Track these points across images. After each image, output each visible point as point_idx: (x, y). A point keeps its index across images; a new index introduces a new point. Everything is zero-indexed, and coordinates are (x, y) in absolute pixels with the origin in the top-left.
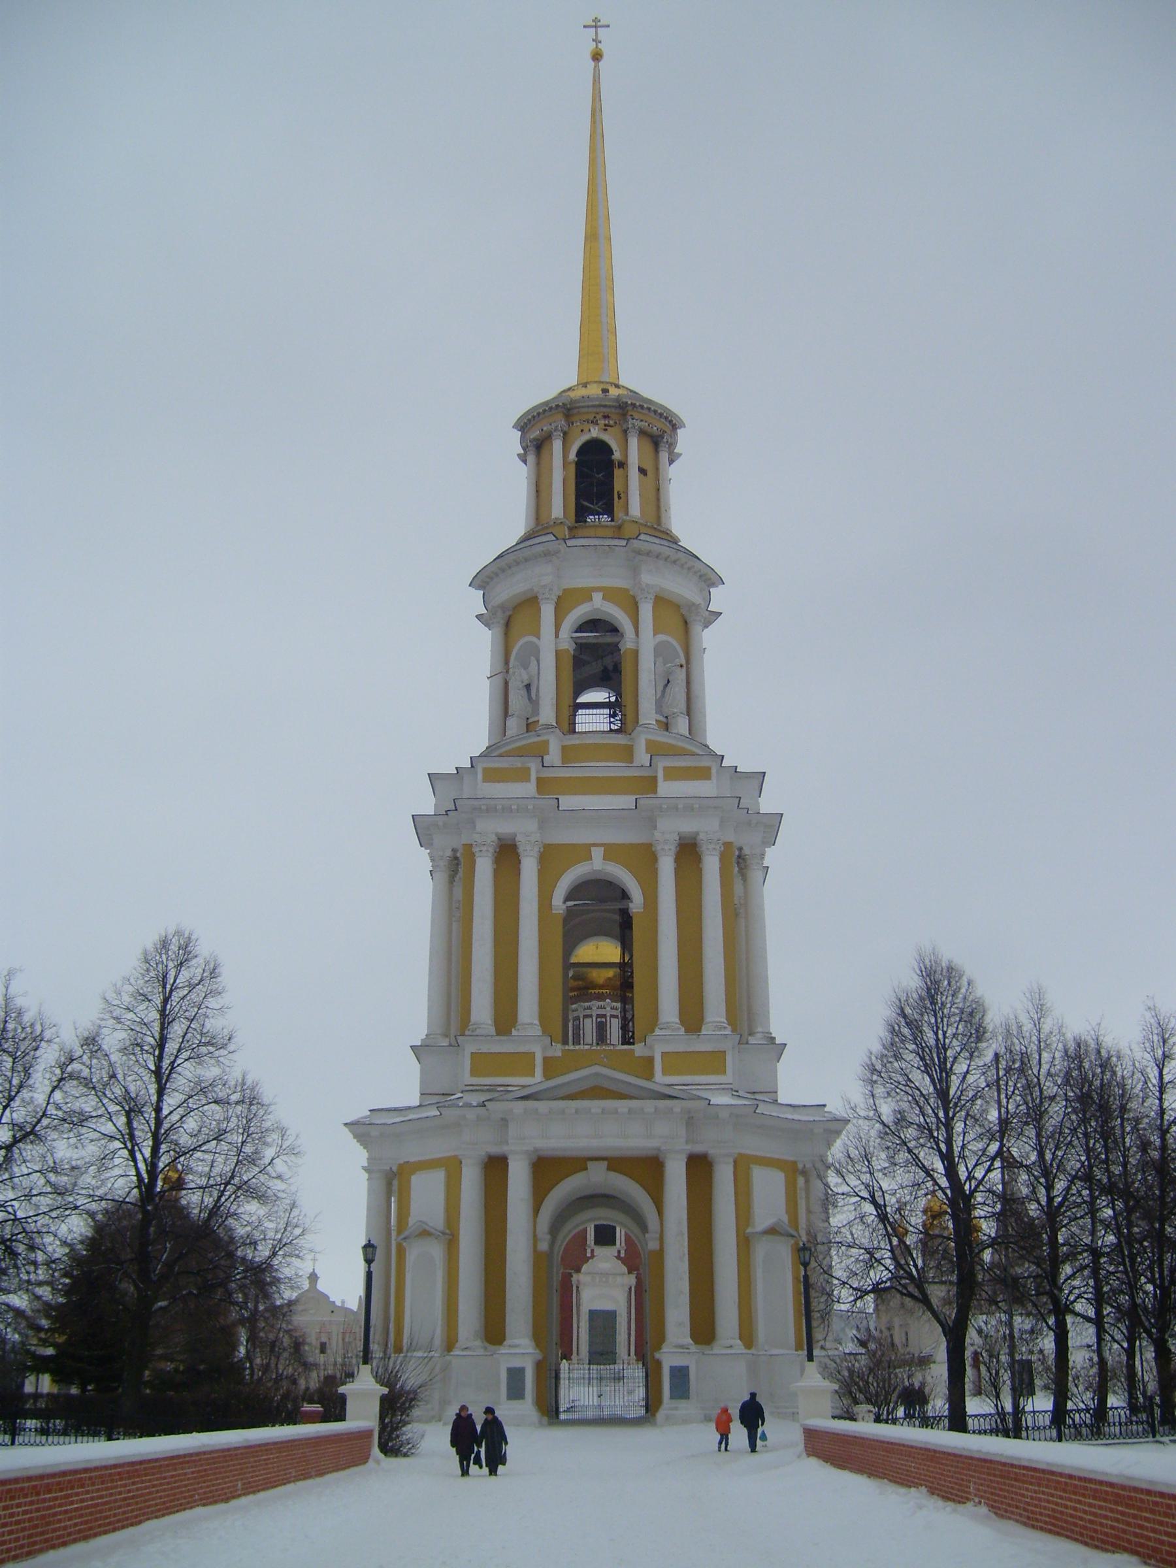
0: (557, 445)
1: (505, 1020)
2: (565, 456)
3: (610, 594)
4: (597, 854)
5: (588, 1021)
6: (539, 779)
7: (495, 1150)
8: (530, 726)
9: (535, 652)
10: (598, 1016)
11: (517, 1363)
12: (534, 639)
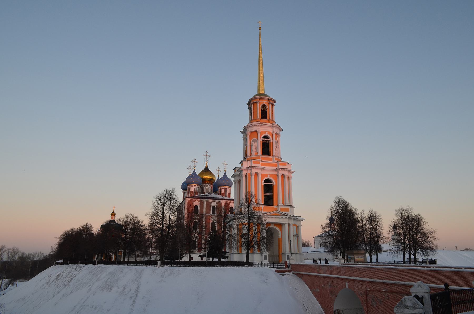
0: (258, 105)
2: (259, 107)
4: (269, 176)
5: (204, 188)
10: (206, 187)
11: (265, 255)
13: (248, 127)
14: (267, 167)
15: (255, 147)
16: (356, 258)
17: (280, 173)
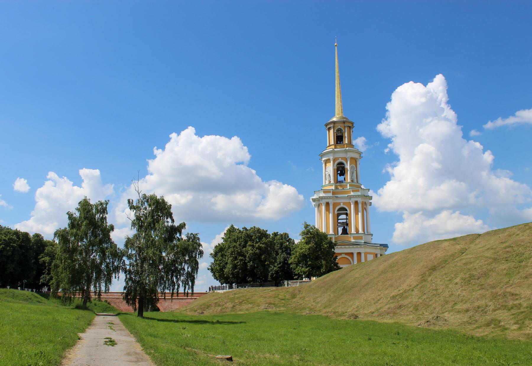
3: (342, 158)
4: (342, 204)
6: (332, 192)
12: (330, 167)
17: (353, 200)
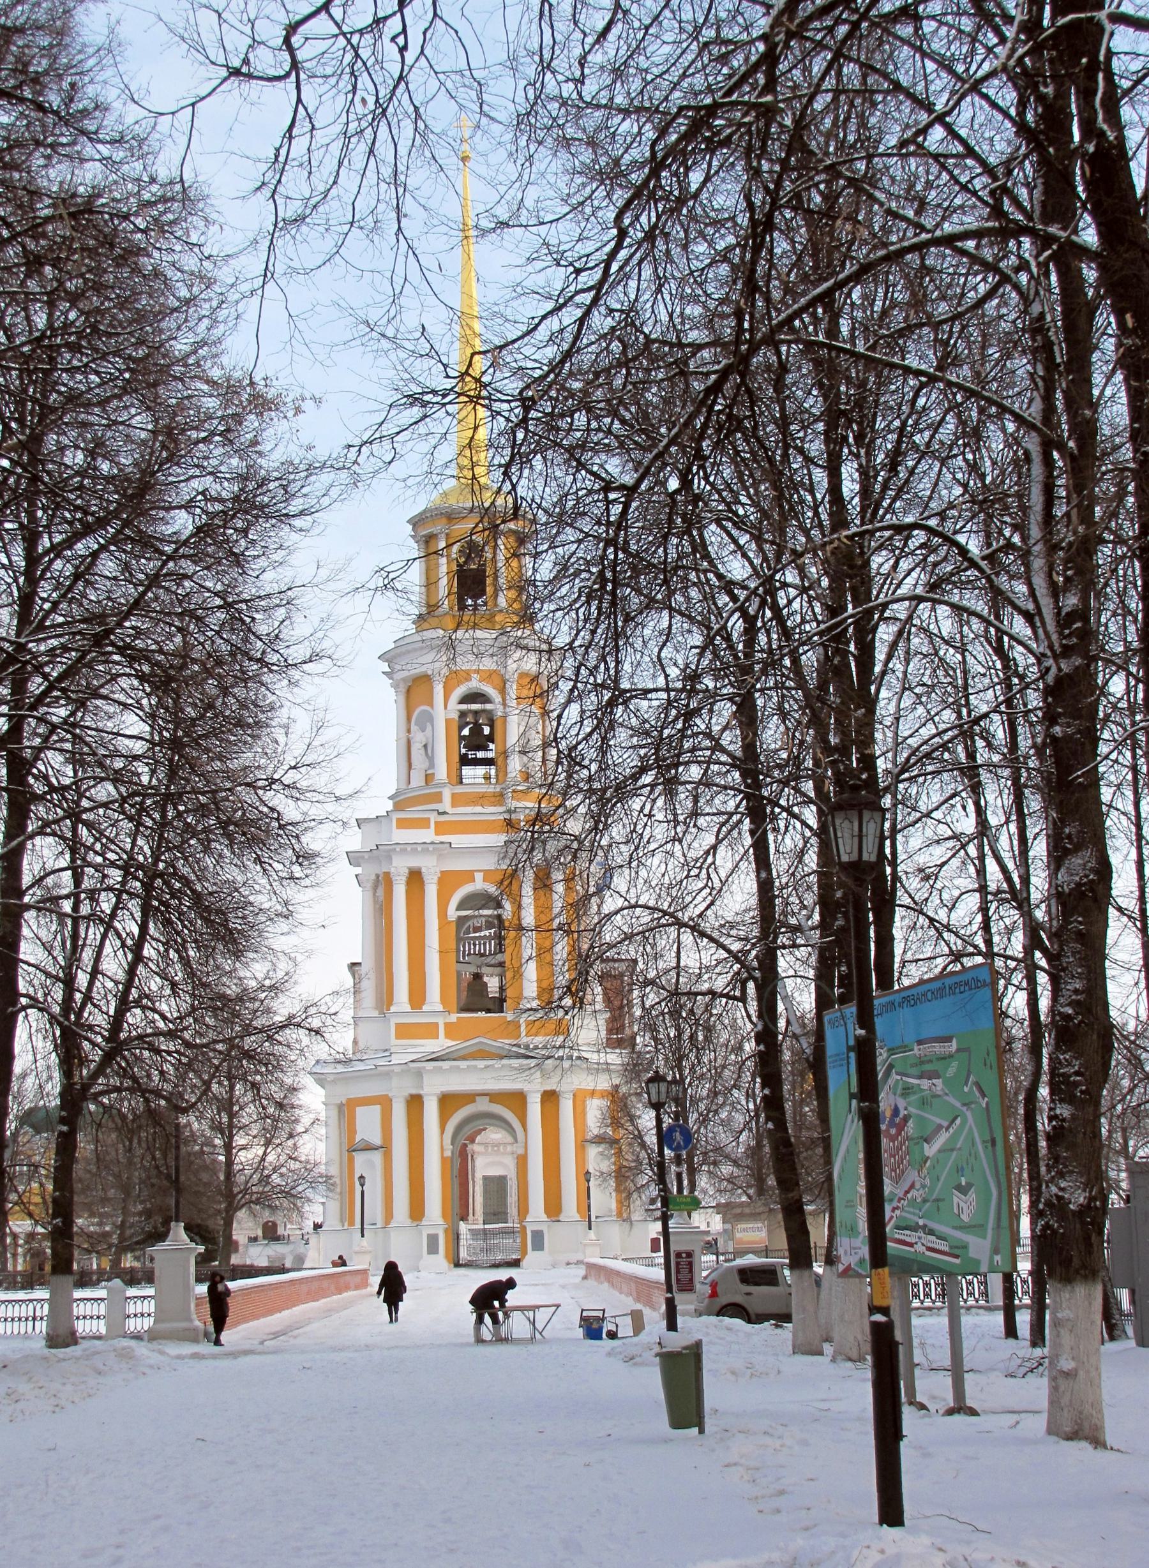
1: (417, 997)
4: (479, 877)
7: (414, 1092)
8: (429, 778)
9: (431, 719)
11: (432, 1231)
13: (399, 655)
14: (457, 840)
15: (425, 746)
16: (738, 1235)
